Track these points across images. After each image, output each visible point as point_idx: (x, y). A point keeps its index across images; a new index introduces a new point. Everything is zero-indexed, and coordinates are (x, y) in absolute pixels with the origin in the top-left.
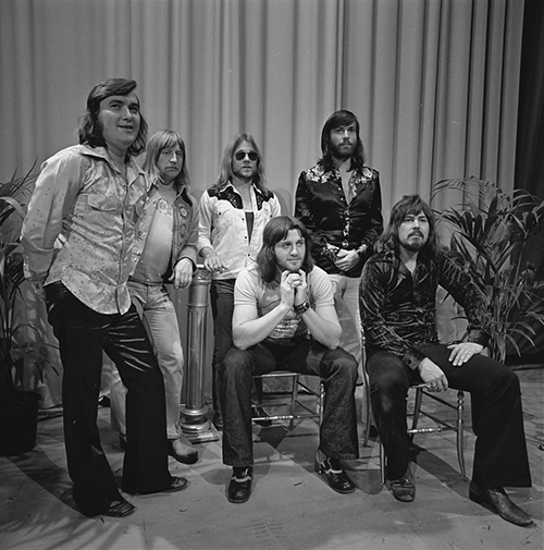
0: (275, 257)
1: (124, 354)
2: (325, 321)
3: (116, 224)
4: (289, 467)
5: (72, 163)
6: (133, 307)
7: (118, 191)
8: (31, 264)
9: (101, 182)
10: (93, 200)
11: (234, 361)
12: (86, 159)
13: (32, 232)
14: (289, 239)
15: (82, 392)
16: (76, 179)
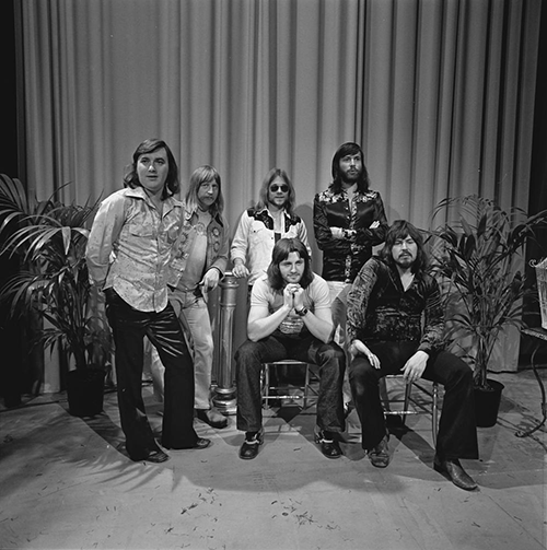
0: (279, 271)
1: (161, 342)
2: (322, 322)
3: (152, 246)
4: (295, 437)
5: (118, 203)
6: (169, 305)
8: (93, 275)
9: (140, 216)
10: (132, 228)
11: (247, 351)
12: (129, 200)
13: (91, 252)
14: (289, 260)
15: (133, 364)
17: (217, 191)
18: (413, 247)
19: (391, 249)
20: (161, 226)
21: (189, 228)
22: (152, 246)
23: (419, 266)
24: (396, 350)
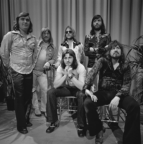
2: (80, 82)
3: (23, 50)
7: (24, 41)
9: (18, 39)
10: (15, 44)
12: (13, 34)
16: (10, 39)
17: (49, 35)
18: (119, 51)
19: (110, 52)
20: (27, 43)
21: (39, 48)
22: (23, 50)
23: (121, 59)
24: (109, 95)
